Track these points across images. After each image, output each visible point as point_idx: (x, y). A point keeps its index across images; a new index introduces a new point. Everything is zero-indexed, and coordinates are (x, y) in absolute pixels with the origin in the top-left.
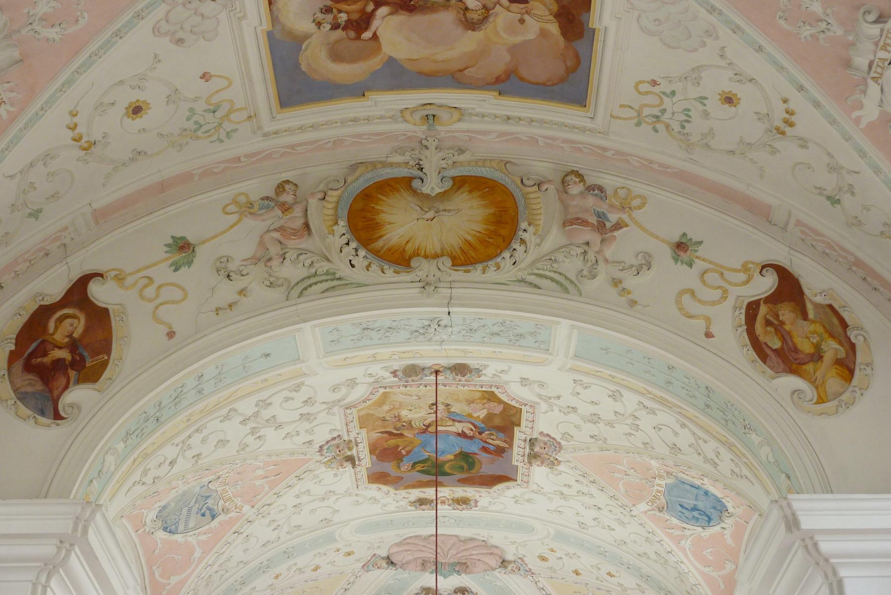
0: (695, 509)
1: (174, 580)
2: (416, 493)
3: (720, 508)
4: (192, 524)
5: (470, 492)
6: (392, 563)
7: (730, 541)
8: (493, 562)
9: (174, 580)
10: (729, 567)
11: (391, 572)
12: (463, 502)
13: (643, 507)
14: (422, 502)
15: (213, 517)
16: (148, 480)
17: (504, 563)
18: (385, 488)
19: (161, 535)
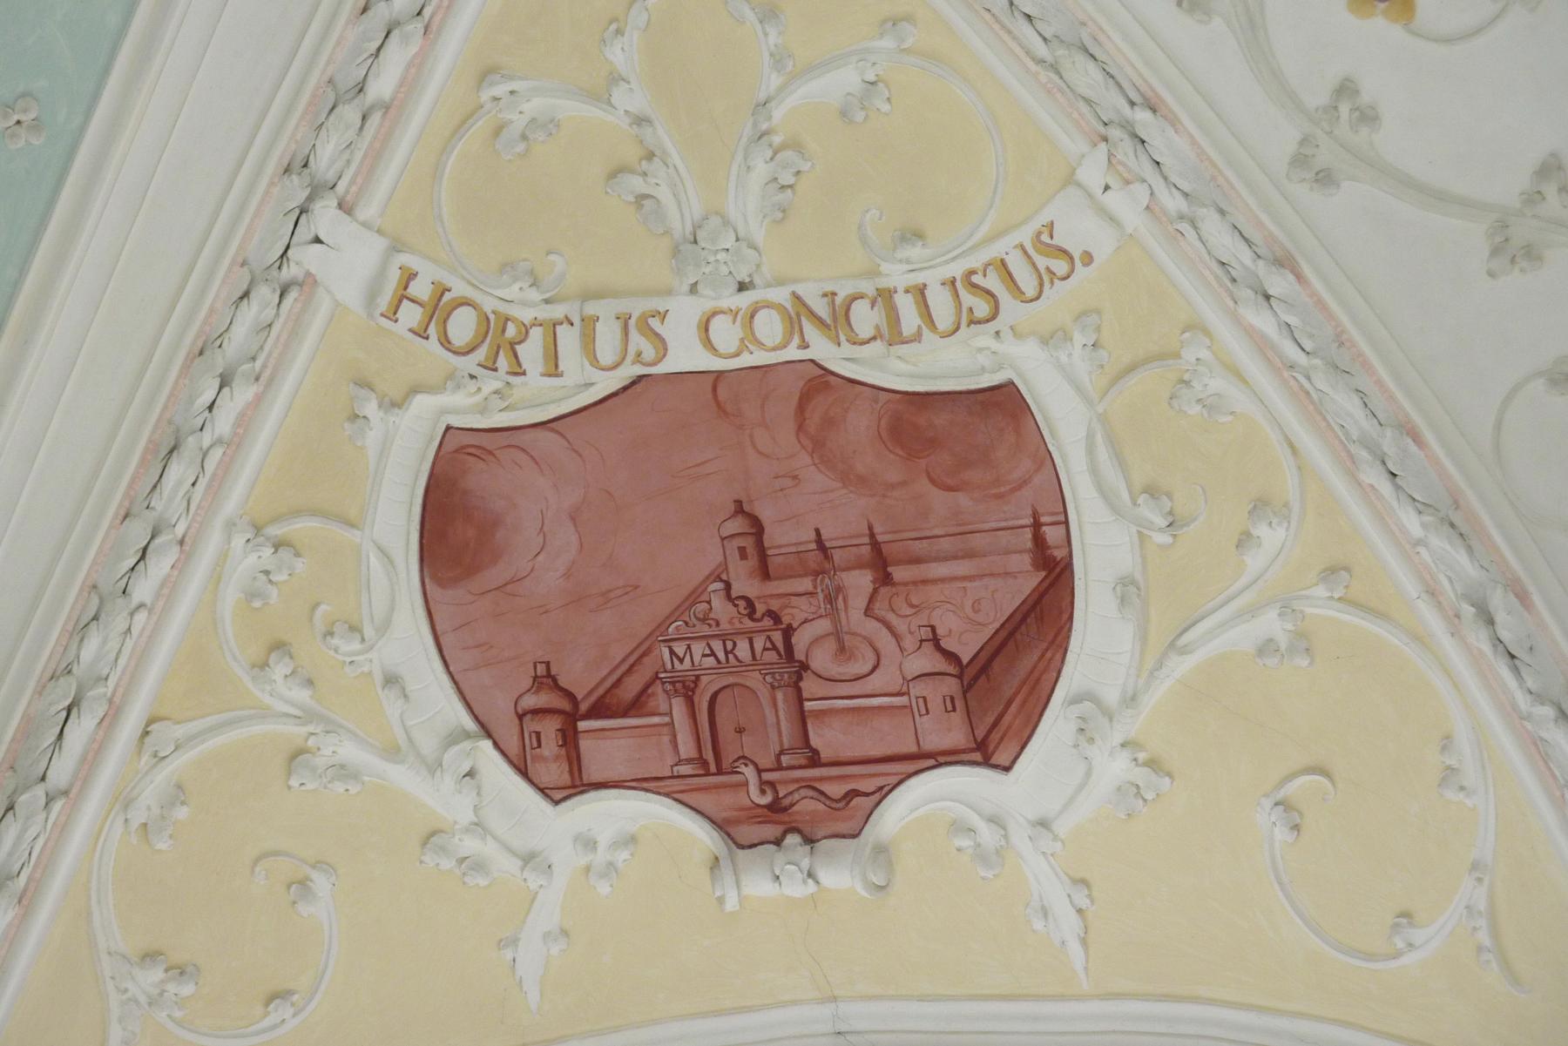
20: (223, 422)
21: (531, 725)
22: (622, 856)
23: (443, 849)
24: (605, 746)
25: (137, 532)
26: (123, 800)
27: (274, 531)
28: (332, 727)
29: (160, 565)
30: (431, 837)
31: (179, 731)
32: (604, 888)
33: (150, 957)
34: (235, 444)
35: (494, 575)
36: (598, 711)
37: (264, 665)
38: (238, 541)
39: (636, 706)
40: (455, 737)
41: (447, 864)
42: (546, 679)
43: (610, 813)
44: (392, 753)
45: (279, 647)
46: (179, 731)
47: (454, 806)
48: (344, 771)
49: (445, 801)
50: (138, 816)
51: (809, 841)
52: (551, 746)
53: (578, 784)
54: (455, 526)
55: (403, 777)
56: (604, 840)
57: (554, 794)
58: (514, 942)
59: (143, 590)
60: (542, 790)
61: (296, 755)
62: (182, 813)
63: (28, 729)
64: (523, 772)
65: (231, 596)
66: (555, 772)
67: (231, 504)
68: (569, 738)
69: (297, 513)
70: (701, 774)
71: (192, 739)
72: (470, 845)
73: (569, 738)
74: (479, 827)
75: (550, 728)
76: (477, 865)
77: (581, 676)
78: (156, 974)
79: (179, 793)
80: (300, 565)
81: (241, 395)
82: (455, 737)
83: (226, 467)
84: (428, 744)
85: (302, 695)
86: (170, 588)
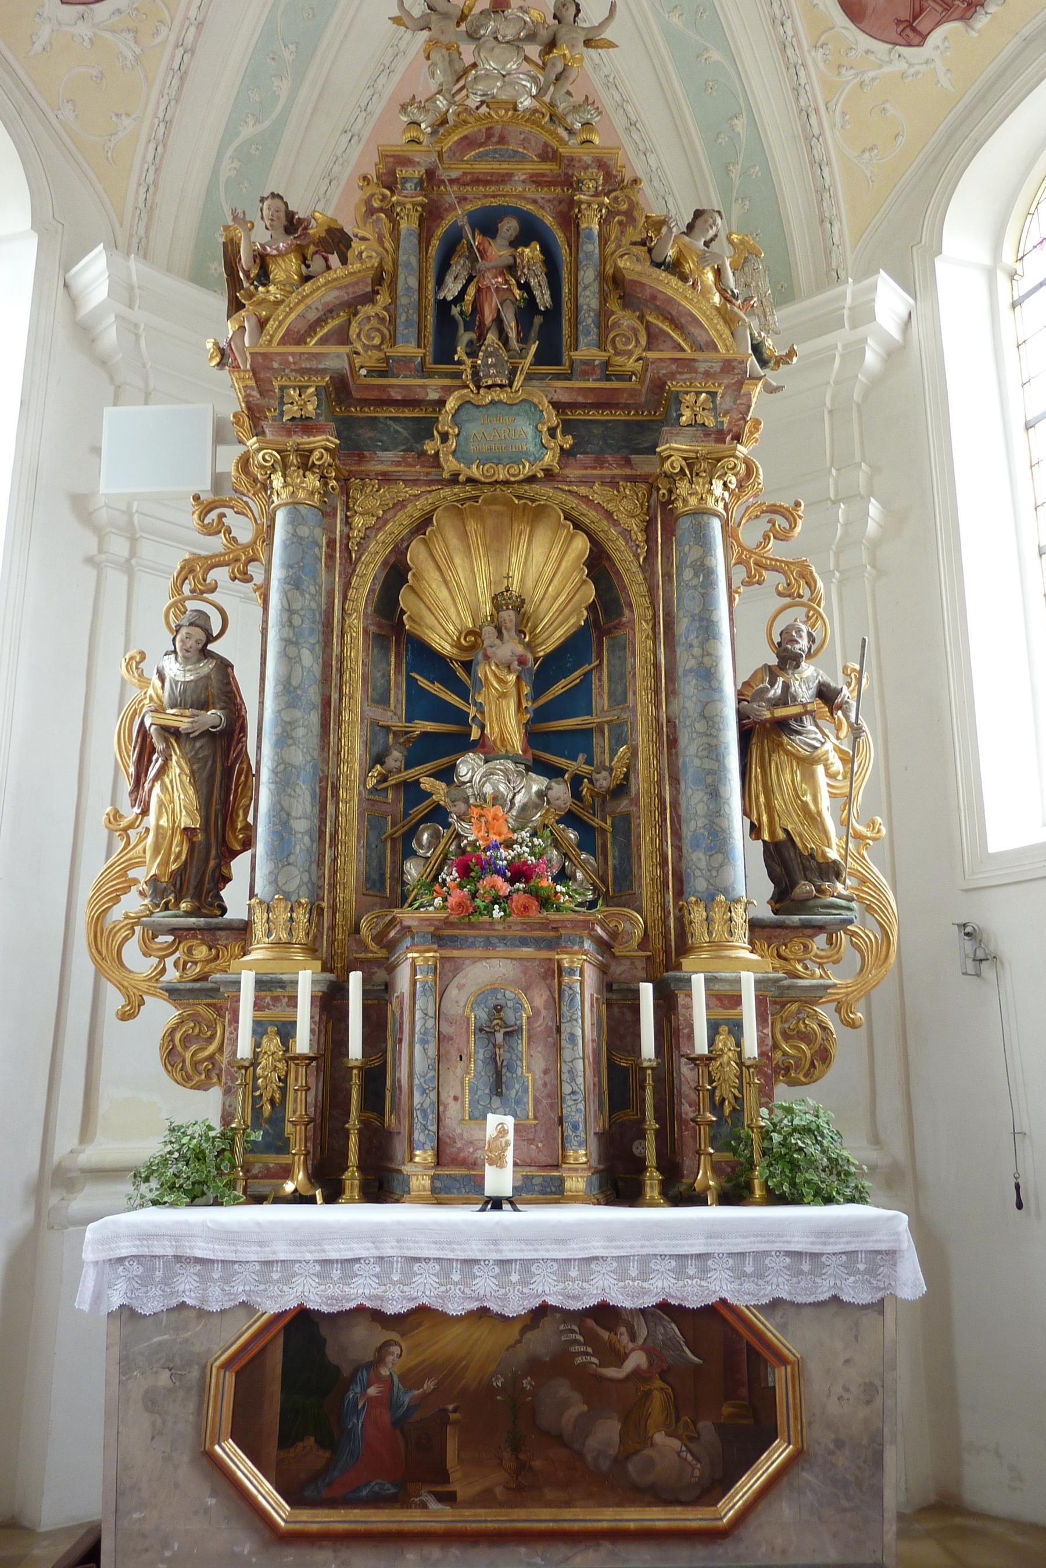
20: (790, 33)
21: (904, 34)
22: (946, 44)
23: (907, 77)
24: (922, 24)
25: (792, 71)
26: (833, 125)
27: (819, 44)
28: (863, 73)
29: (802, 73)
30: (903, 76)
31: (834, 101)
32: (949, 54)
33: (863, 151)
34: (796, 34)
35: (869, 11)
36: (915, 18)
37: (839, 73)
38: (813, 53)
39: (922, 10)
40: (890, 52)
41: (910, 79)
42: (899, 22)
43: (935, 38)
44: (880, 67)
45: (840, 66)
46: (834, 101)
47: (900, 66)
48: (873, 79)
49: (900, 66)
50: (839, 125)
51: (982, 5)
52: (912, 35)
53: (924, 37)
55: (886, 69)
56: (940, 43)
57: (920, 45)
58: (938, 81)
59: (803, 81)
60: (918, 45)
61: (861, 84)
62: (847, 117)
63: (804, 130)
64: (910, 45)
65: (821, 64)
66: (917, 40)
67: (806, 47)
68: (914, 30)
69: (820, 37)
71: (837, 102)
72: (912, 70)
73: (914, 30)
74: (911, 65)
75: (908, 31)
76: (917, 73)
77: (905, 14)
78: (867, 154)
79: (844, 114)
80: (829, 46)
81: (788, 24)
82: (890, 52)
83: (798, 41)
84: (886, 58)
85: (852, 71)
86: (808, 76)
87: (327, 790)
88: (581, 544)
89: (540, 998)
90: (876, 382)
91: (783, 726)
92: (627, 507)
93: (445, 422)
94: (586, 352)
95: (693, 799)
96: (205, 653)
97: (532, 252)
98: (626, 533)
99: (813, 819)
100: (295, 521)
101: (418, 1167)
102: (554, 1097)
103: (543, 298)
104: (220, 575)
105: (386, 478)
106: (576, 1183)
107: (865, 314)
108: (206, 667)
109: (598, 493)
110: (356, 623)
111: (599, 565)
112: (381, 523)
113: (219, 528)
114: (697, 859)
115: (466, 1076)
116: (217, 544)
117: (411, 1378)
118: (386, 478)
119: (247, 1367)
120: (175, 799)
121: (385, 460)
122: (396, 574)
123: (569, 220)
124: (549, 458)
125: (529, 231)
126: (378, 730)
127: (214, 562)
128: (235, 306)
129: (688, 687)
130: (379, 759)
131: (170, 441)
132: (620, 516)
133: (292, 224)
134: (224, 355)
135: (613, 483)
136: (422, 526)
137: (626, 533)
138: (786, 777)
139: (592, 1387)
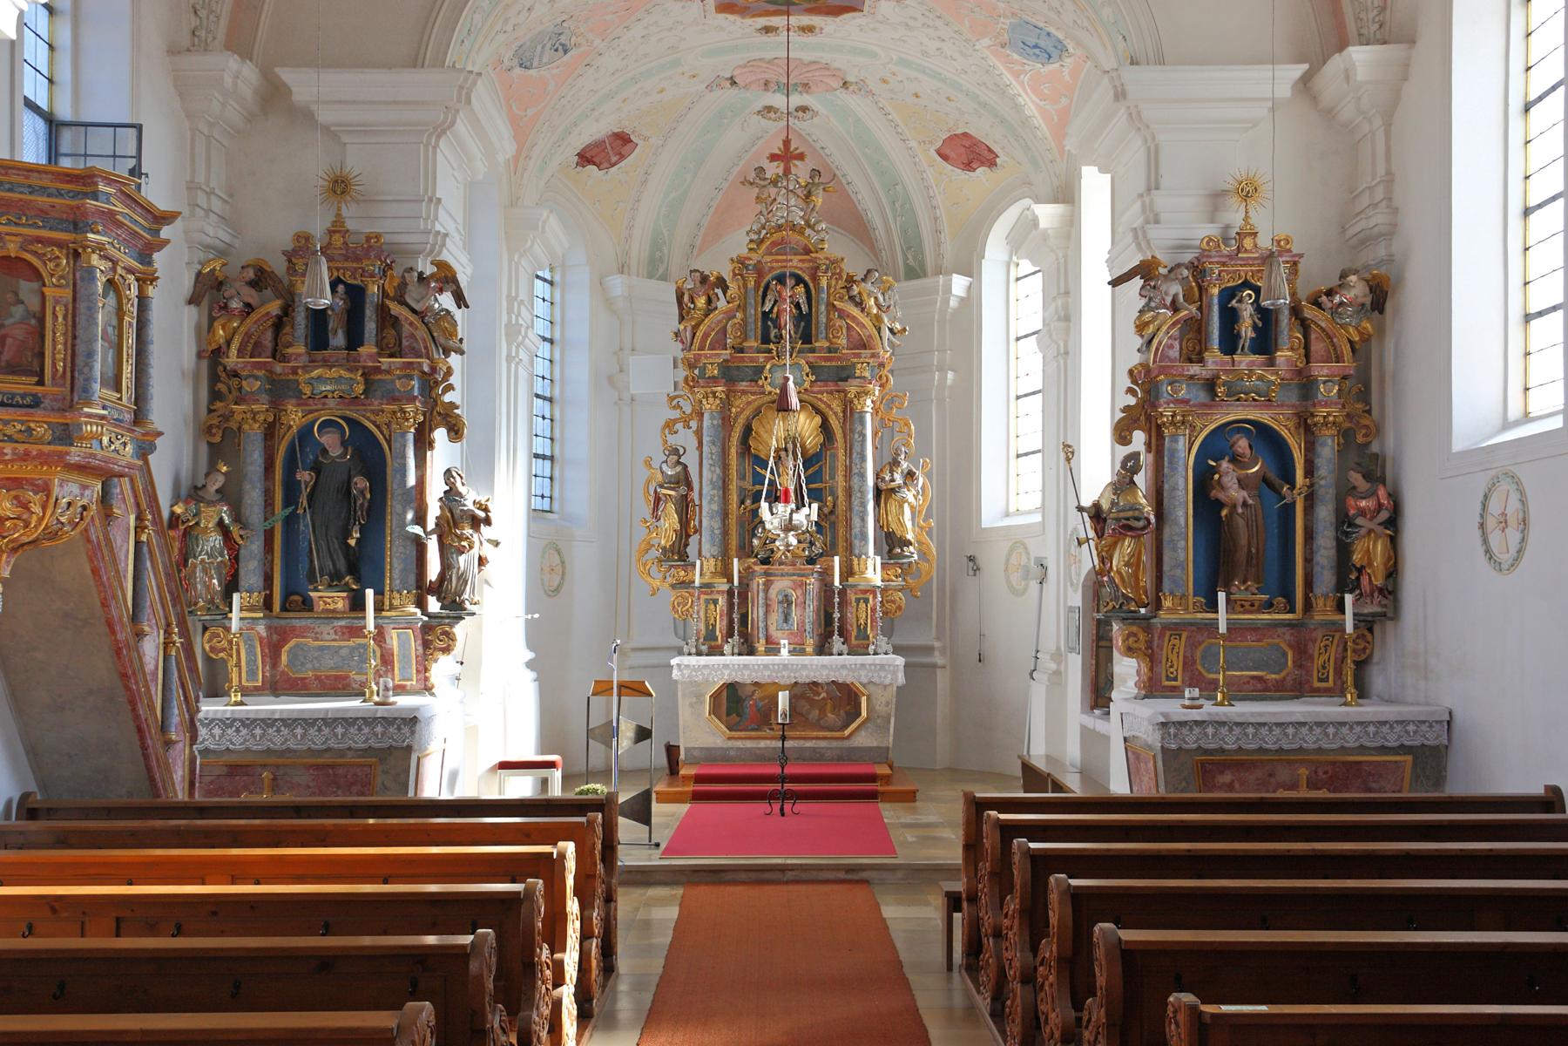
0: (1036, 46)
1: (530, 112)
2: (763, 21)
3: (1062, 49)
4: (545, 59)
5: (816, 20)
6: (734, 83)
7: (1067, 78)
8: (836, 84)
9: (530, 112)
10: (1064, 101)
11: (734, 91)
12: (809, 29)
13: (986, 42)
14: (767, 30)
15: (566, 52)
16: (509, 28)
17: (845, 84)
18: (731, 17)
19: (518, 71)
54: (945, 157)
70: (983, 164)
87: (725, 515)
88: (818, 420)
89: (799, 592)
90: (957, 311)
91: (893, 491)
92: (837, 406)
93: (766, 373)
94: (821, 343)
95: (856, 522)
96: (678, 463)
97: (801, 289)
98: (836, 414)
99: (902, 525)
100: (712, 418)
101: (761, 646)
102: (802, 624)
103: (805, 308)
104: (679, 426)
105: (744, 392)
106: (809, 649)
107: (948, 289)
108: (679, 468)
109: (825, 397)
110: (733, 451)
111: (825, 427)
112: (743, 410)
113: (678, 406)
114: (856, 542)
115: (776, 617)
116: (676, 414)
117: (761, 699)
118: (744, 392)
119: (715, 697)
120: (670, 520)
121: (743, 385)
122: (748, 430)
123: (815, 278)
124: (807, 385)
125: (799, 280)
126: (741, 490)
127: (675, 421)
128: (682, 318)
129: (856, 479)
130: (742, 502)
131: (656, 371)
132: (834, 406)
133: (704, 279)
134: (677, 334)
135: (831, 393)
136: (758, 412)
137: (836, 414)
138: (893, 507)
139: (810, 701)
